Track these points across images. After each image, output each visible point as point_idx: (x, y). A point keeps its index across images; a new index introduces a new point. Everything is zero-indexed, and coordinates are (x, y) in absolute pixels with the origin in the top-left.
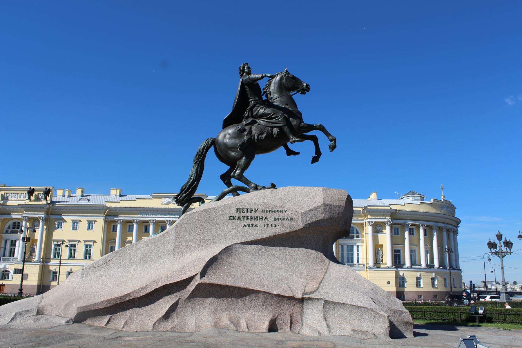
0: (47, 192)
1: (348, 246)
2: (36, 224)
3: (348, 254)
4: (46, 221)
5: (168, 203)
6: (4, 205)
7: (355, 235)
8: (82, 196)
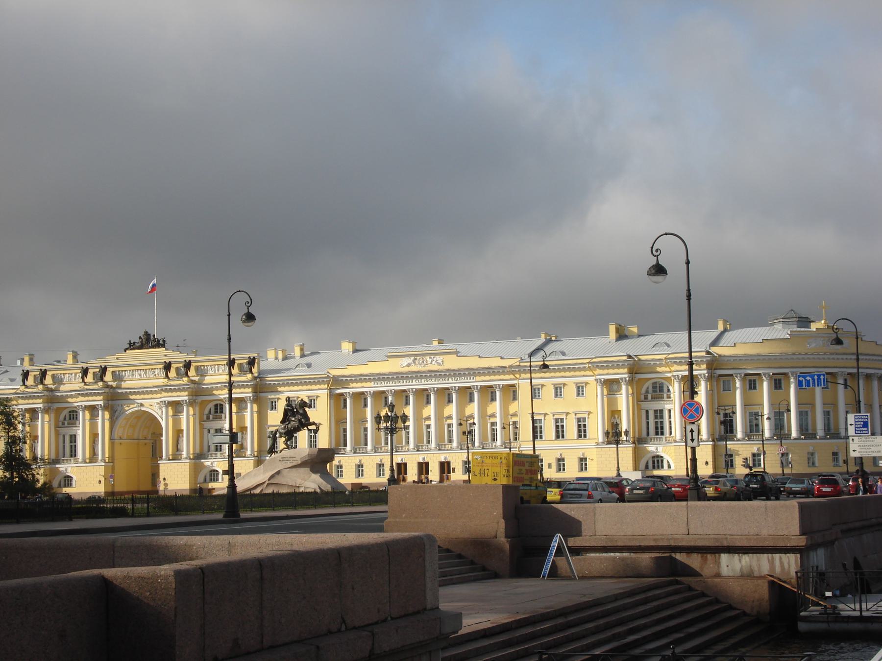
0: (252, 362)
1: (656, 411)
2: (244, 406)
3: (656, 423)
4: (256, 399)
5: (409, 365)
6: (200, 383)
7: (665, 395)
8: (303, 356)
